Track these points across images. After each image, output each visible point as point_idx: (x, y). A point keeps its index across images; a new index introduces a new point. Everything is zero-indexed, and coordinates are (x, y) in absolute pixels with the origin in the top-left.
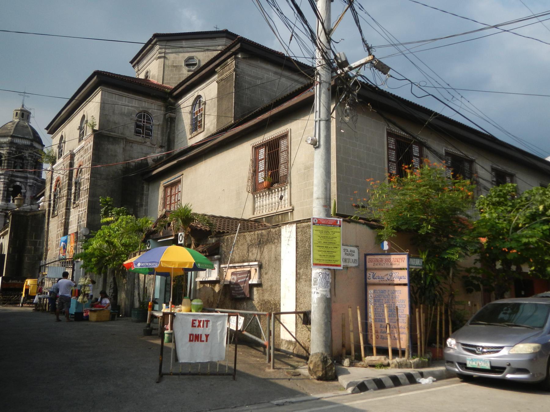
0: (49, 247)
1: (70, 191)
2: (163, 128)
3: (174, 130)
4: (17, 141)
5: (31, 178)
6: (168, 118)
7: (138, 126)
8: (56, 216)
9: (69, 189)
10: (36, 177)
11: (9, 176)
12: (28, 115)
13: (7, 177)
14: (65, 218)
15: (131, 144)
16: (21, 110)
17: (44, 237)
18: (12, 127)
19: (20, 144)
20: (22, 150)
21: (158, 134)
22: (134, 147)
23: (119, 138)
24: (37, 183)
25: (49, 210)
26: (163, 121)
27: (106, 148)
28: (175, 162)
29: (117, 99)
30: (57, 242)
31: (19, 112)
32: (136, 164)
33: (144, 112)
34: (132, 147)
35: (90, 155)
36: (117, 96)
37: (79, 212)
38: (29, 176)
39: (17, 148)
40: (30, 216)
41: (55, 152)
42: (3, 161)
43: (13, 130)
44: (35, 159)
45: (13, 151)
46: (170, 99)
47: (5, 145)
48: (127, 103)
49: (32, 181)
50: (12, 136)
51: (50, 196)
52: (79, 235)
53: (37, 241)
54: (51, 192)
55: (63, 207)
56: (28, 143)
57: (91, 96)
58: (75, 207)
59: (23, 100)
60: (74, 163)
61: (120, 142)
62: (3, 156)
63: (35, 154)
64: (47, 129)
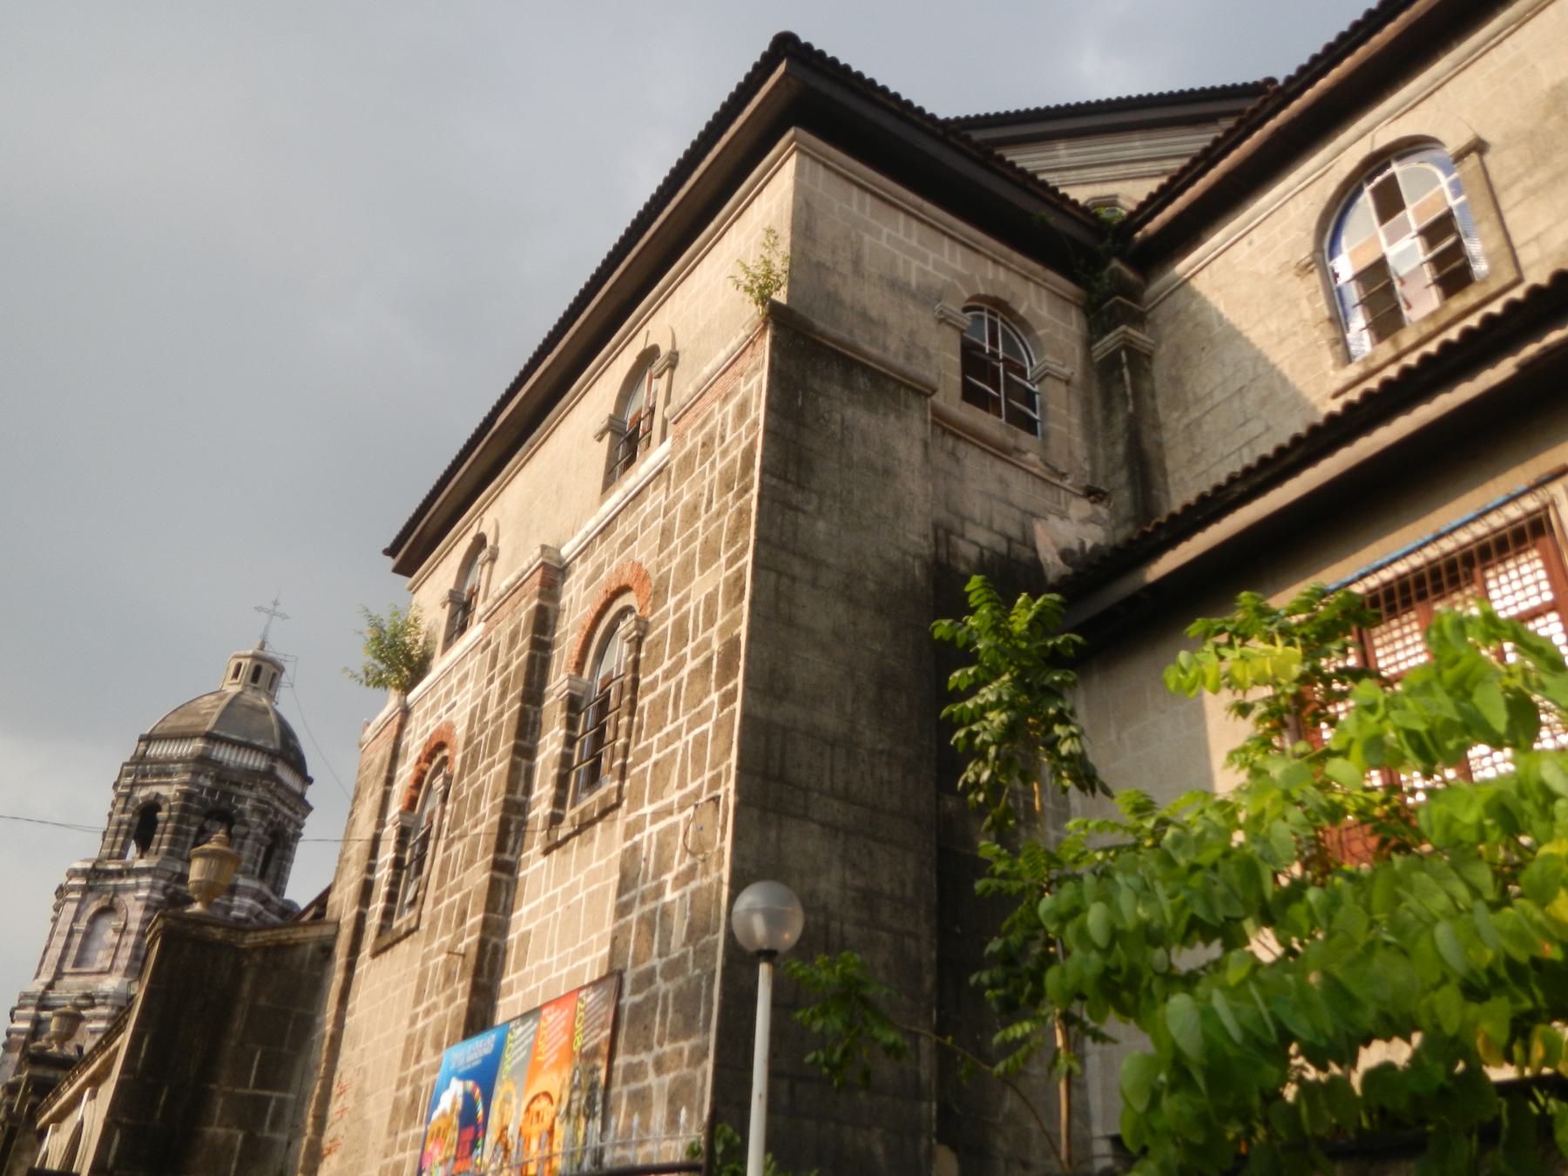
0: (329, 1135)
1: (524, 762)
2: (1087, 403)
3: (1155, 411)
4: (224, 754)
5: (247, 892)
6: (1116, 354)
7: (973, 361)
8: (409, 932)
9: (525, 750)
10: (266, 890)
11: (169, 879)
12: (274, 675)
13: (162, 883)
14: (486, 925)
15: (950, 442)
16: (254, 657)
17: (308, 1073)
18: (216, 706)
19: (232, 765)
20: (233, 789)
21: (1069, 425)
22: (968, 462)
23: (901, 384)
24: (266, 912)
25: (360, 920)
26: (1086, 373)
27: (838, 417)
28: (1503, 370)
29: (868, 209)
30: (407, 1091)
31: (248, 661)
32: (982, 554)
33: (990, 312)
34: (958, 460)
35: (737, 452)
36: (868, 198)
37: (633, 829)
38: (242, 881)
39: (219, 779)
40: (255, 948)
41: (424, 627)
42: (160, 825)
43: (215, 718)
44: (271, 823)
45: (201, 787)
46: (1116, 263)
47: (179, 765)
48: (914, 243)
49: (248, 902)
50: (210, 737)
51: (375, 842)
52: (628, 1000)
53: (269, 1099)
54: (381, 824)
55: (470, 862)
56: (257, 762)
57: (712, 226)
58: (567, 839)
59: (267, 628)
60: (558, 613)
61: (907, 407)
62: (165, 807)
63: (277, 803)
64: (391, 551)
